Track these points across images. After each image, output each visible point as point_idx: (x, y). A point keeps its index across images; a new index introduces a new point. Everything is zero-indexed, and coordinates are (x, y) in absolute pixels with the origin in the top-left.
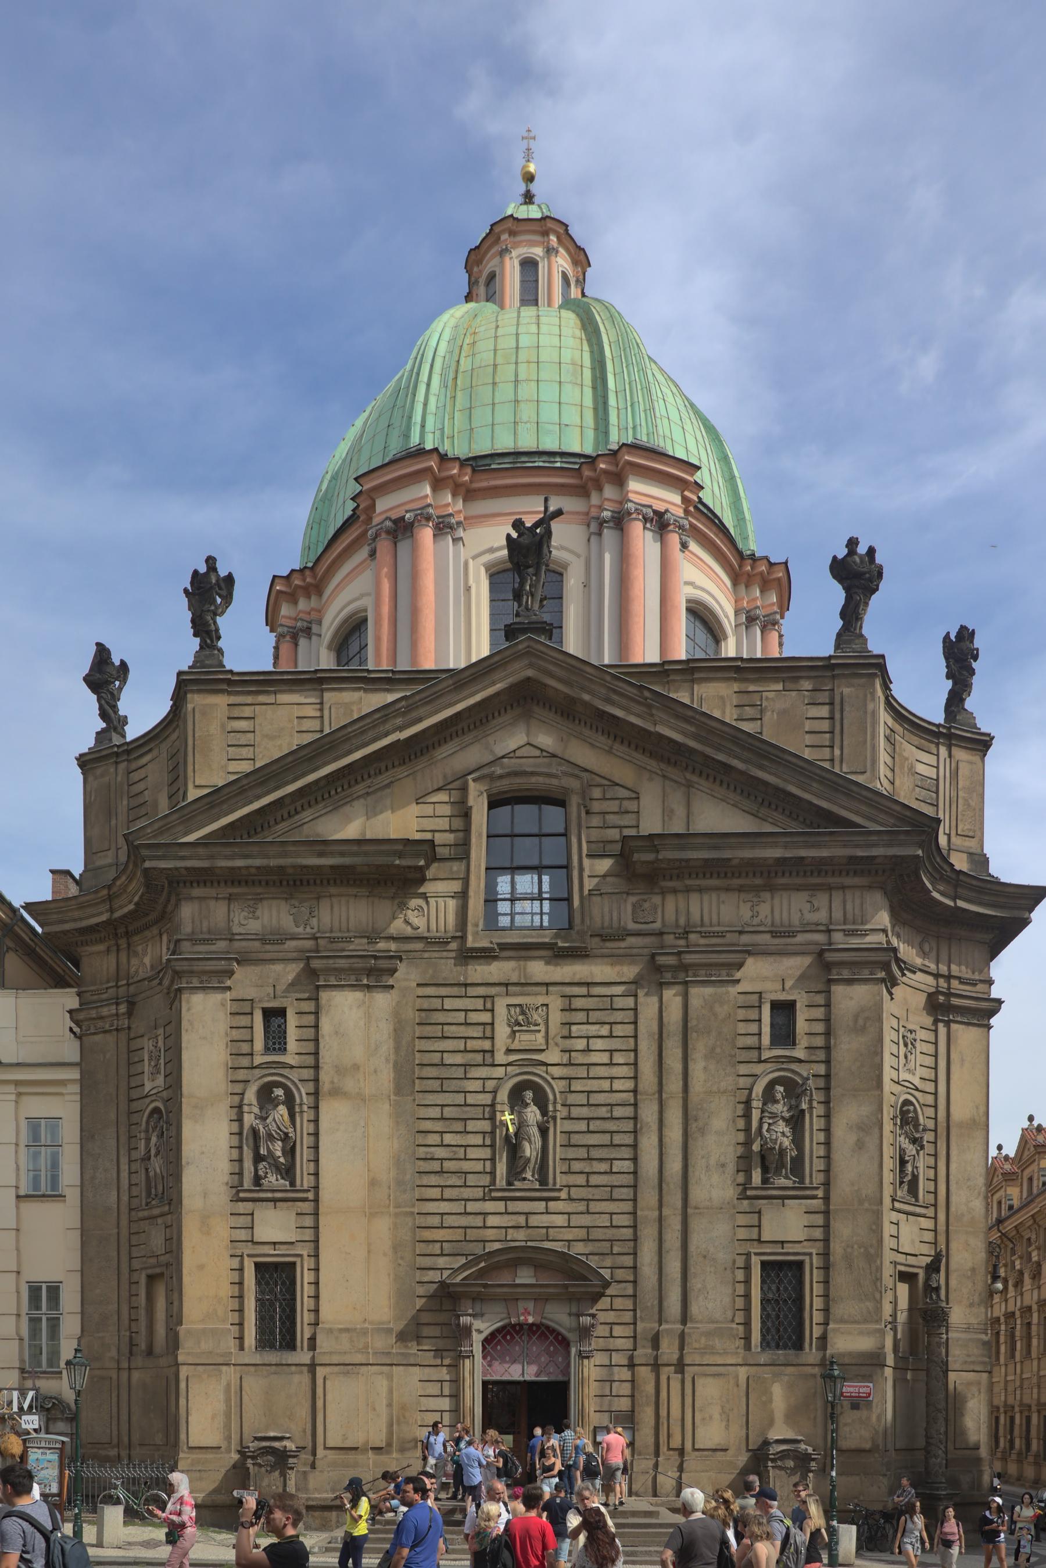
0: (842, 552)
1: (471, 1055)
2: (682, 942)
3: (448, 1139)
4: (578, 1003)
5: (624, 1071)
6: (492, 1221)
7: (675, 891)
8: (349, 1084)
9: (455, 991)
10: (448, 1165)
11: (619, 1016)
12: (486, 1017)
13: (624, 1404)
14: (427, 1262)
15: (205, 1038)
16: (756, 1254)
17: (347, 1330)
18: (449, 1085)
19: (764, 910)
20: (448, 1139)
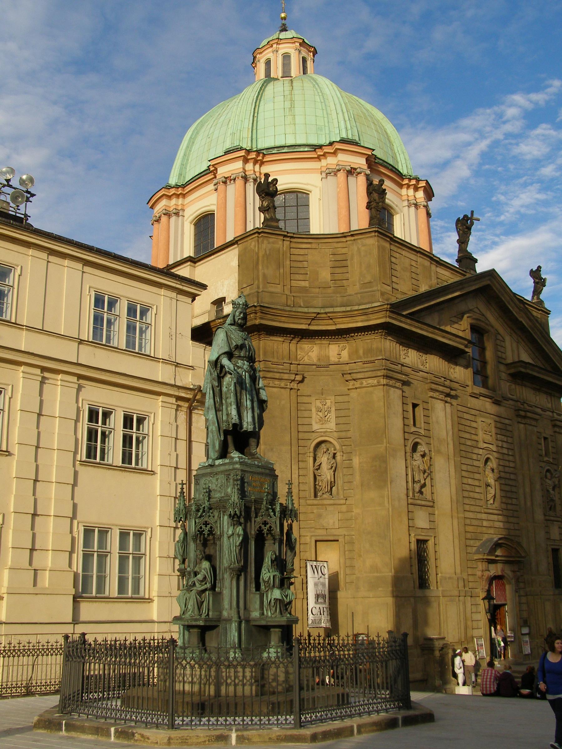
0: (535, 269)
1: (473, 442)
2: (522, 406)
3: (470, 481)
5: (511, 458)
6: (485, 523)
7: (519, 384)
8: (443, 449)
10: (472, 494)
11: (508, 434)
12: (474, 425)
13: (525, 615)
14: (468, 542)
15: (394, 413)
16: (550, 545)
17: (450, 578)
18: (470, 455)
19: (538, 398)
20: (470, 481)
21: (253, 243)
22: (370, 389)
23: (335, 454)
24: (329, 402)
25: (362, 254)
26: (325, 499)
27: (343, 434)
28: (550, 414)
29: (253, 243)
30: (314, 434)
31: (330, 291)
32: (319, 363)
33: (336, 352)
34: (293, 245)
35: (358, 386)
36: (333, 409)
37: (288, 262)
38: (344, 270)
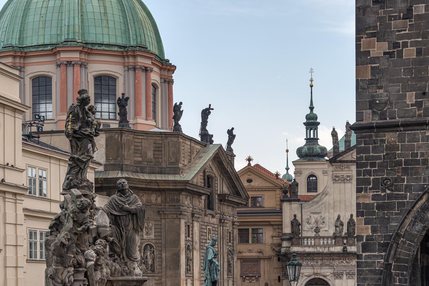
0: (230, 129)
4: (214, 229)
9: (202, 223)
11: (216, 233)
12: (205, 231)
21: (117, 135)
22: (173, 220)
23: (153, 251)
24: (151, 225)
25: (170, 145)
26: (149, 273)
27: (158, 241)
28: (232, 218)
29: (117, 135)
30: (144, 241)
31: (152, 164)
32: (147, 204)
33: (155, 199)
34: (136, 137)
35: (166, 217)
36: (153, 228)
37: (133, 147)
38: (160, 153)
